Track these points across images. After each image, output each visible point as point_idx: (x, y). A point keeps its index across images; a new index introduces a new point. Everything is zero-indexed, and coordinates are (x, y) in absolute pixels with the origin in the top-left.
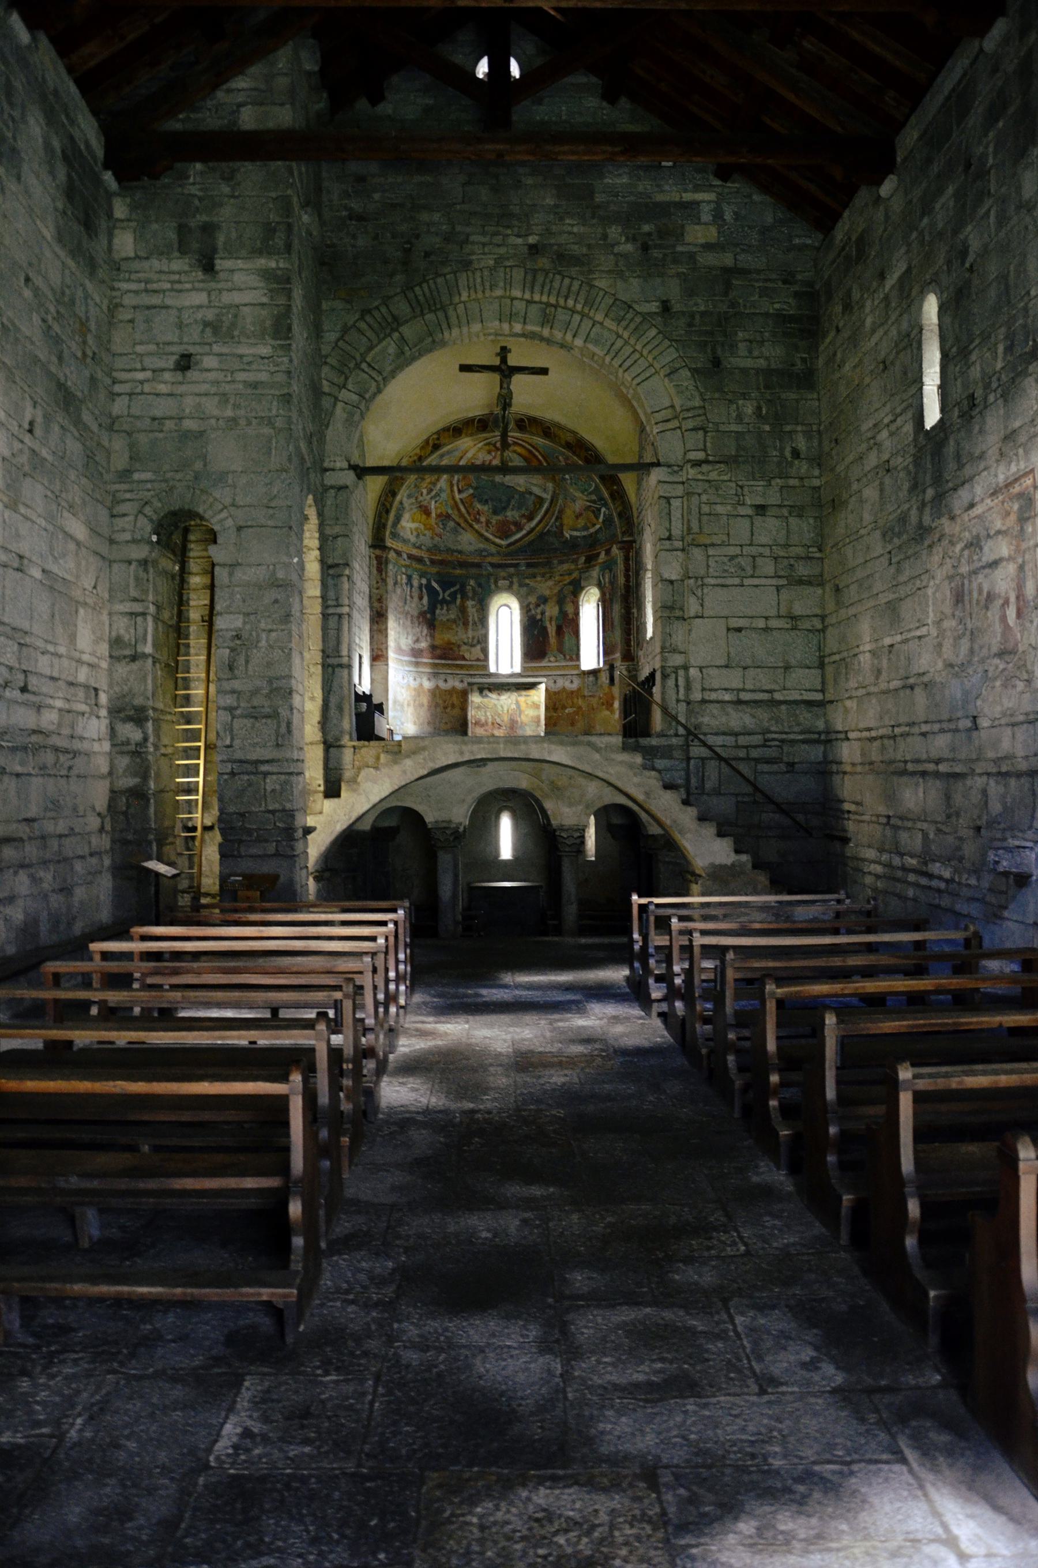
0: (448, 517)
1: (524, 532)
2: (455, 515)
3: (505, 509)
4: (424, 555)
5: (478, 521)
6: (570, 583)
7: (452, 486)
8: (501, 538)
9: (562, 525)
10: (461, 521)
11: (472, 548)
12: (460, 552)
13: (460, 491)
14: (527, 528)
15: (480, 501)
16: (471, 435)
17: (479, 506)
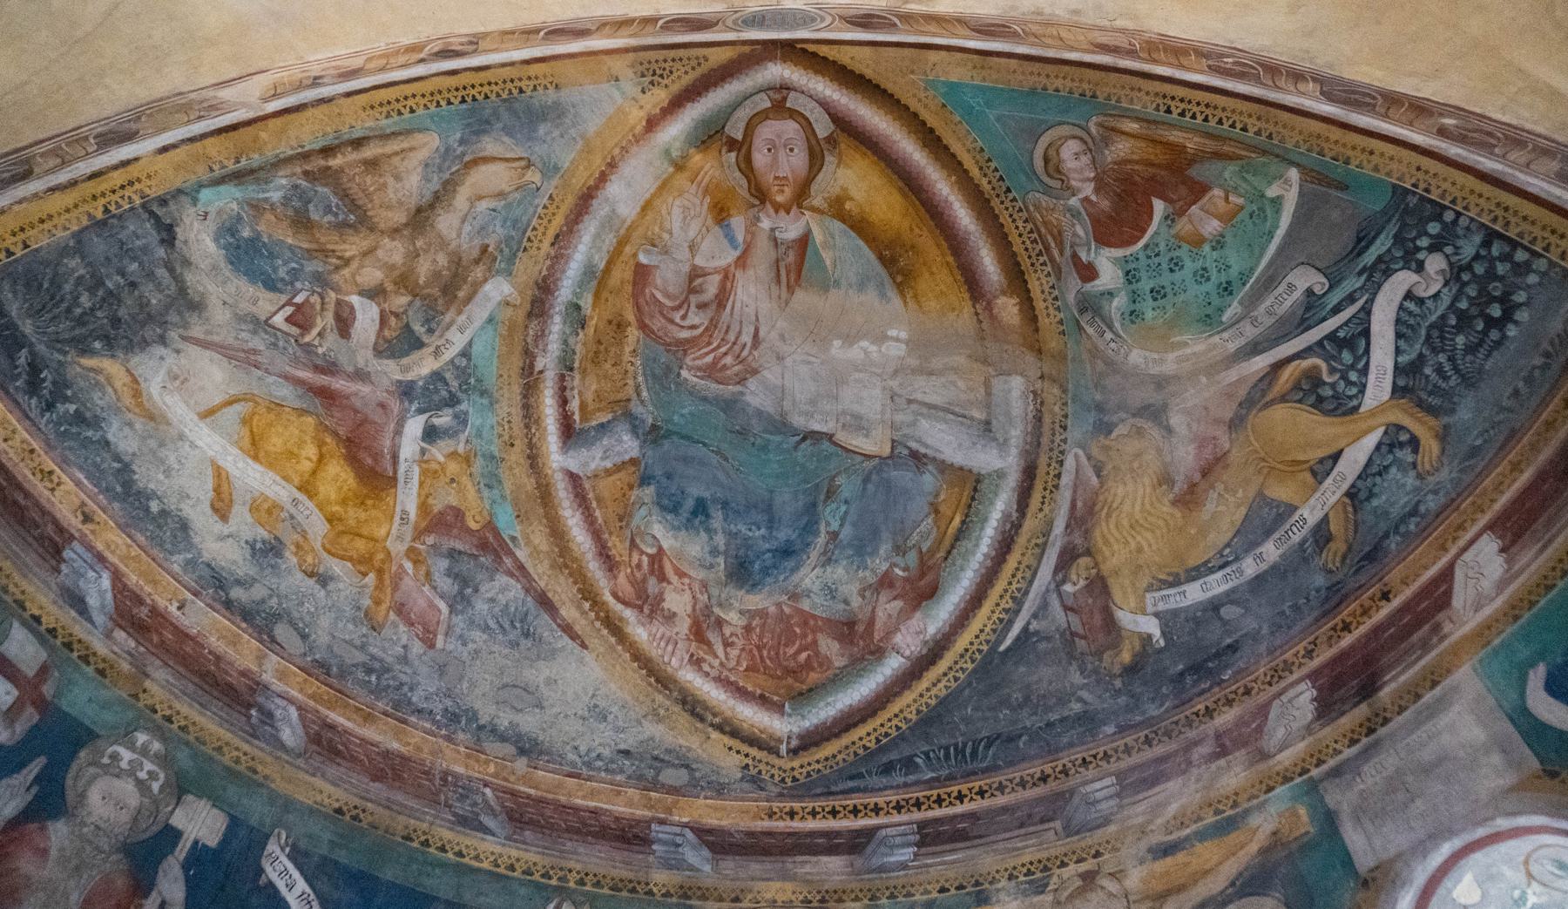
0: (492, 545)
1: (892, 665)
2: (530, 546)
3: (786, 552)
4: (270, 670)
5: (650, 606)
6: (1252, 882)
7: (530, 387)
8: (763, 701)
9: (1099, 586)
10: (562, 591)
11: (602, 740)
12: (528, 748)
13: (569, 433)
14: (910, 640)
15: (669, 505)
16: (631, 36)
17: (662, 533)
